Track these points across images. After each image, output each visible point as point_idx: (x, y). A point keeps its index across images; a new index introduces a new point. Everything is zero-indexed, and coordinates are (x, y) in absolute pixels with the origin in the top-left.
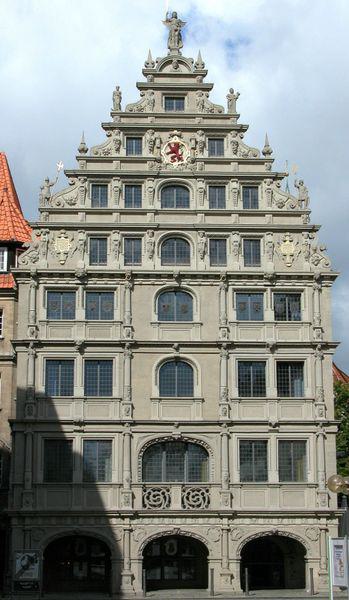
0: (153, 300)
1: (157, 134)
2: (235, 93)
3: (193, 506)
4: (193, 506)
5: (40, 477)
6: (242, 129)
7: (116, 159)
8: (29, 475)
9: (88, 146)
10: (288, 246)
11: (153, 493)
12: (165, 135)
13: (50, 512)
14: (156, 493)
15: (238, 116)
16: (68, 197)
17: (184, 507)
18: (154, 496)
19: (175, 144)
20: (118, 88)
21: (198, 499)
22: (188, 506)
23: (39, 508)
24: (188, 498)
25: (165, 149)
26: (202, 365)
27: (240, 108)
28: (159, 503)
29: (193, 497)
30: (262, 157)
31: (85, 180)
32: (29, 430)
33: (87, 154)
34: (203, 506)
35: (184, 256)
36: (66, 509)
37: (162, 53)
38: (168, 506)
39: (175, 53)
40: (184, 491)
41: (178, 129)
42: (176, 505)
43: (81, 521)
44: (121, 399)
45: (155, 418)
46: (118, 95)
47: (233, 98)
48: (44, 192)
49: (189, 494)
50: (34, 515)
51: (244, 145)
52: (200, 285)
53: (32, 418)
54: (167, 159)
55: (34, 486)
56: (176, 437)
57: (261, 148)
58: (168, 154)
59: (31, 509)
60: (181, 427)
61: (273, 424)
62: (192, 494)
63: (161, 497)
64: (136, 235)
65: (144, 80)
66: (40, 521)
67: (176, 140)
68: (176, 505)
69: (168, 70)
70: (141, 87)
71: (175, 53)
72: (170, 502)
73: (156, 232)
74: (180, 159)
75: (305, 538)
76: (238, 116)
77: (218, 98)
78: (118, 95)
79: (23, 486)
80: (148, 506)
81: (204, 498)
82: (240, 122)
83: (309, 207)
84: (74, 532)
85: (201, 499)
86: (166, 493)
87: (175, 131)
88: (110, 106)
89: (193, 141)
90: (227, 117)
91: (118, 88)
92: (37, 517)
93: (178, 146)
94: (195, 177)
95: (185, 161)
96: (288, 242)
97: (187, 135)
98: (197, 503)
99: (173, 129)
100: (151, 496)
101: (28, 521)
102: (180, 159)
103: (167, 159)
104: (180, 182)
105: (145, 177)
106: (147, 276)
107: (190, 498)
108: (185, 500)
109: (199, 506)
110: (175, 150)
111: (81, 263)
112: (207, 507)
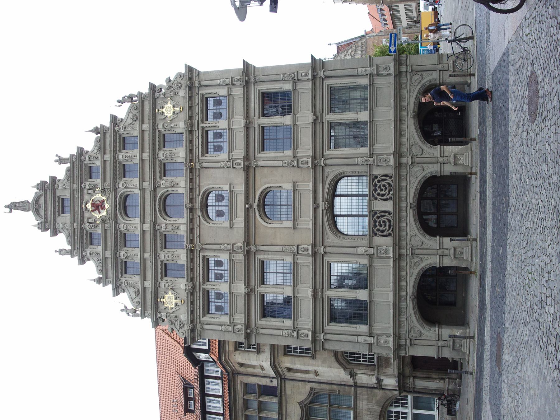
0: (212, 225)
1: (85, 220)
3: (390, 190)
4: (390, 190)
5: (364, 328)
7: (104, 254)
8: (361, 339)
9: (97, 276)
10: (168, 110)
11: (378, 227)
12: (86, 215)
13: (394, 321)
14: (377, 224)
17: (391, 198)
18: (381, 226)
19: (92, 206)
20: (56, 251)
22: (390, 195)
23: (391, 332)
24: (383, 195)
25: (97, 215)
26: (265, 183)
27: (66, 156)
28: (387, 221)
29: (382, 190)
31: (120, 280)
32: (321, 337)
34: (390, 181)
36: (392, 307)
38: (389, 213)
40: (376, 199)
41: (81, 204)
42: (389, 206)
43: (403, 294)
44: (294, 255)
45: (310, 226)
46: (61, 252)
47: (61, 161)
49: (378, 194)
50: (397, 336)
51: (93, 151)
52: (199, 185)
53: (310, 333)
54: (104, 213)
55: (371, 335)
56: (327, 206)
57: (94, 136)
58: (99, 213)
59: (391, 339)
60: (318, 202)
61: (314, 118)
62: (379, 191)
63: (382, 219)
64: (161, 240)
66: (403, 331)
67: (89, 206)
68: (389, 206)
69: (42, 212)
73: (158, 222)
74: (103, 201)
75: (419, 86)
77: (61, 172)
78: (61, 252)
79: (370, 345)
80: (390, 232)
81: (383, 180)
84: (413, 300)
85: (384, 183)
86: (378, 215)
87: (83, 206)
89: (90, 191)
91: (56, 251)
92: (399, 334)
93: (93, 205)
94: (116, 190)
95: (104, 198)
96: (164, 110)
97: (86, 197)
99: (81, 208)
100: (381, 228)
101: (403, 342)
102: (103, 201)
103: (104, 213)
104: (120, 202)
105: (116, 230)
106: (192, 230)
107: (382, 193)
108: (384, 198)
110: (98, 206)
111: (182, 284)
112: (391, 177)
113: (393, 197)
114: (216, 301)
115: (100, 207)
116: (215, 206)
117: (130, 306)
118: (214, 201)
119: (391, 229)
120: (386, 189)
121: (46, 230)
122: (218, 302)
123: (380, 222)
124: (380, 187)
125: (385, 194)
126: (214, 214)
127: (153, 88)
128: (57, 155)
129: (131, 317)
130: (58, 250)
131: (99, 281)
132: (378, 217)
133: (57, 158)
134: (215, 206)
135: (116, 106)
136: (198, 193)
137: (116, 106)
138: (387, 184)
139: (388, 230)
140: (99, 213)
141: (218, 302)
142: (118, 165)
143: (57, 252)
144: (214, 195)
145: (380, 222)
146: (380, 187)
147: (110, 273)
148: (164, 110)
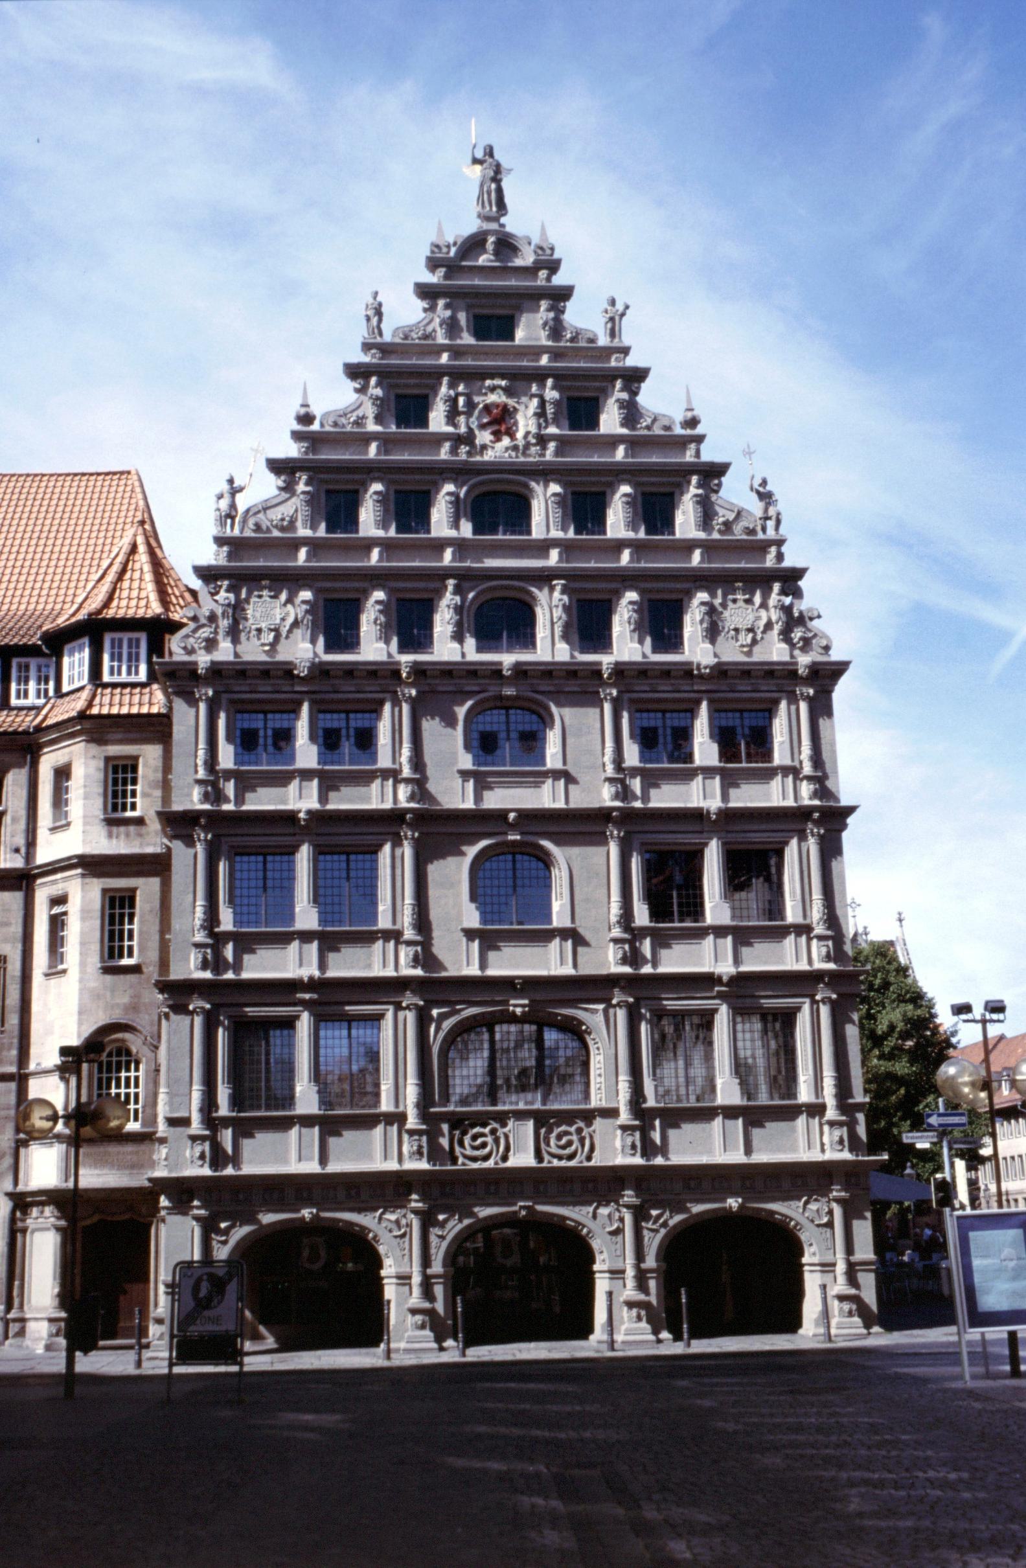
2: (620, 307)
3: (560, 1158)
6: (636, 377)
9: (317, 410)
15: (625, 351)
16: (276, 515)
21: (570, 1143)
30: (678, 430)
33: (316, 427)
35: (524, 633)
37: (470, 225)
39: (494, 226)
48: (224, 504)
57: (679, 416)
65: (433, 278)
70: (426, 292)
71: (494, 226)
72: (507, 1149)
74: (512, 436)
76: (625, 351)
80: (461, 1160)
82: (631, 361)
83: (783, 530)
88: (360, 333)
90: (608, 352)
98: (568, 1151)
109: (571, 1157)
113: (545, 1164)
114: (270, 732)
115: (495, 428)
116: (508, 731)
117: (243, 502)
118: (520, 728)
119: (467, 1162)
120: (564, 1147)
121: (433, 264)
122: (266, 737)
123: (483, 1135)
124: (567, 1133)
125: (548, 1145)
126: (488, 728)
127: (791, 579)
128: (627, 307)
129: (214, 507)
130: (379, 299)
131: (306, 419)
132: (493, 1132)
133: (620, 307)
134: (508, 731)
135: (753, 477)
136: (542, 688)
137: (753, 477)
138: (573, 1148)
139: (465, 1156)
140: (483, 427)
141: (266, 737)
142: (603, 479)
143: (375, 298)
144: (535, 727)
145: (483, 1135)
146: (567, 1133)
147: (328, 455)
148: (741, 604)
